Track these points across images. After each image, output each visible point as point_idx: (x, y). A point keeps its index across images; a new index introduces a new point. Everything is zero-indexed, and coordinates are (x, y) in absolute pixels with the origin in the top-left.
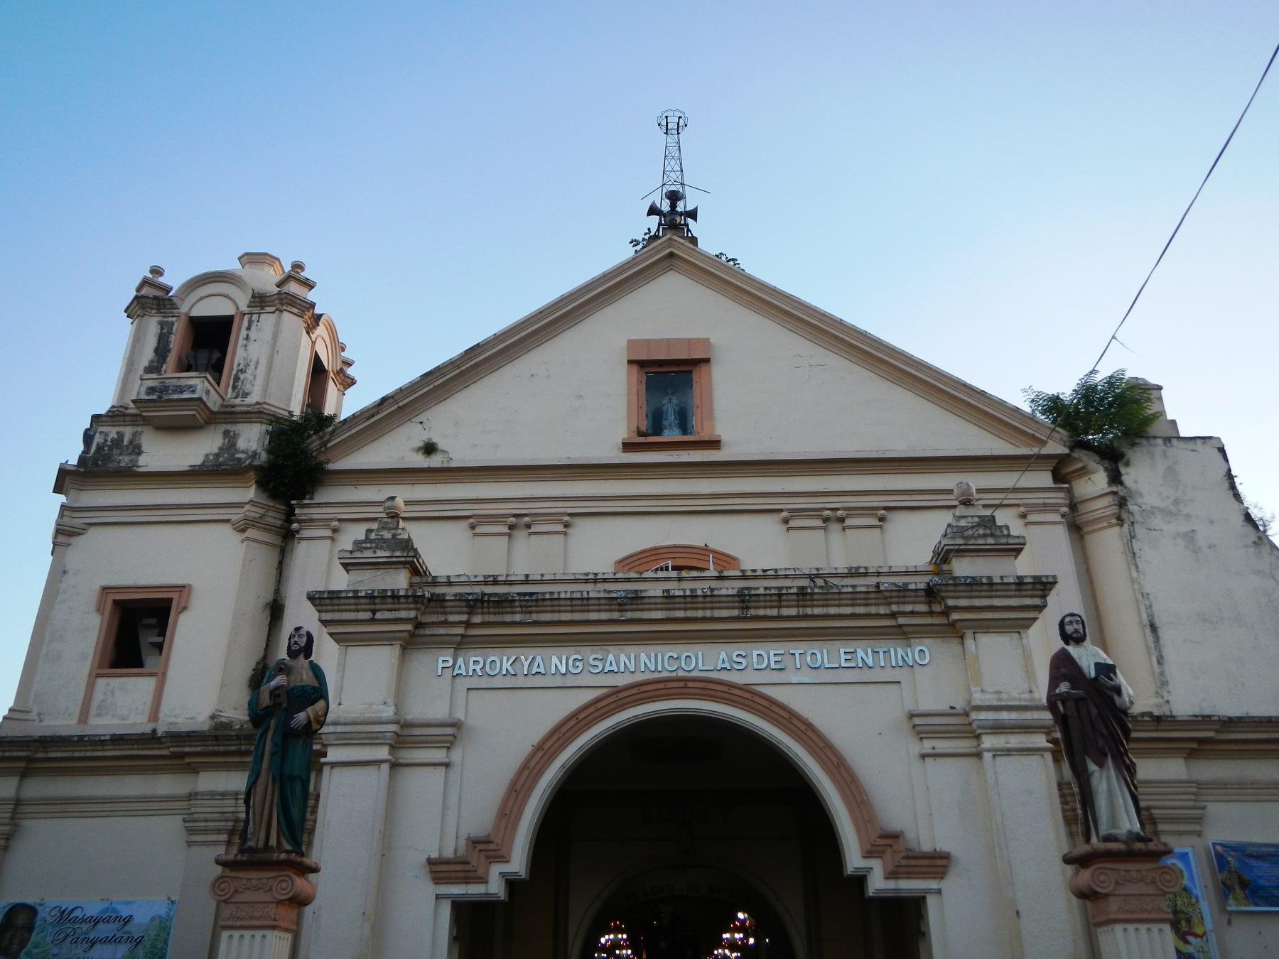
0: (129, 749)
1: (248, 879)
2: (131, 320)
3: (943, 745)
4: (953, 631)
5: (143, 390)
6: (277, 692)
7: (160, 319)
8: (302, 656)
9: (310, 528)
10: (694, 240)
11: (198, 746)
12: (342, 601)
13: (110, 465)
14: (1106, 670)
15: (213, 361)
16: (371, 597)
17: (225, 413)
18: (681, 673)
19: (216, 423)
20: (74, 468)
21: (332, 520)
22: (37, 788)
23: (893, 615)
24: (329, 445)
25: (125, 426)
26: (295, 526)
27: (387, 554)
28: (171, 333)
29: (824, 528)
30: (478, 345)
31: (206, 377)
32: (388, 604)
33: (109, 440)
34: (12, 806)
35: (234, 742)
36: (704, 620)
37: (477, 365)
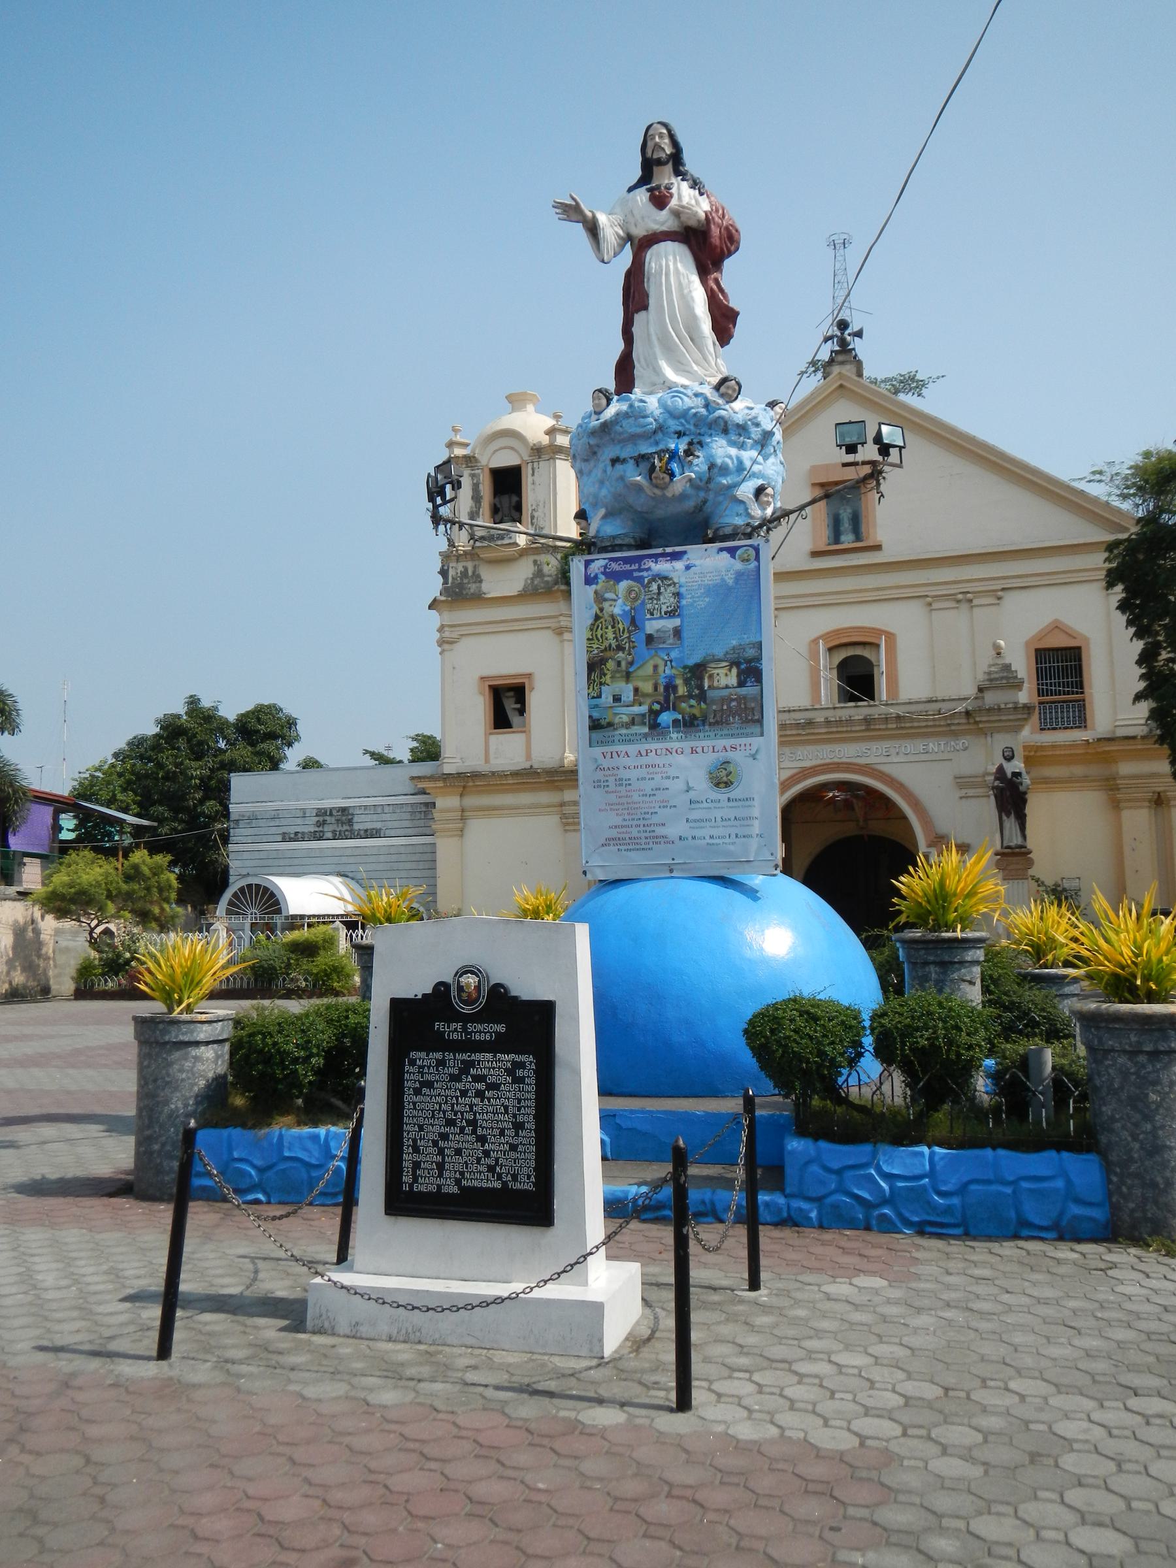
3: (971, 792)
4: (983, 732)
10: (859, 365)
14: (1017, 775)
15: (513, 503)
18: (836, 760)
22: (471, 801)
23: (949, 725)
29: (957, 608)
36: (847, 732)
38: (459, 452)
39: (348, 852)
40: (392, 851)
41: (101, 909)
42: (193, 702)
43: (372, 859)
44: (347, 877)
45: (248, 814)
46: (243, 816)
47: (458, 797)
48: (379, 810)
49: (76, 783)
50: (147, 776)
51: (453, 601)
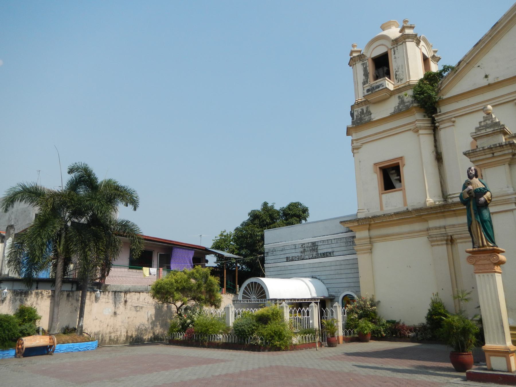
0: (401, 217)
1: (480, 257)
2: (352, 67)
5: (365, 91)
6: (470, 192)
7: (361, 63)
8: (474, 178)
9: (445, 123)
11: (425, 212)
12: (478, 152)
13: (362, 121)
16: (490, 148)
17: (396, 90)
19: (394, 95)
20: (352, 126)
21: (452, 118)
22: (375, 232)
24: (441, 89)
25: (363, 106)
26: (437, 124)
27: (492, 129)
28: (367, 67)
30: (497, 23)
31: (386, 79)
32: (498, 149)
33: (359, 112)
34: (369, 240)
35: (439, 209)
37: (499, 32)
38: (355, 55)
39: (317, 265)
40: (338, 263)
41: (173, 297)
42: (265, 204)
43: (328, 268)
44: (316, 278)
45: (271, 249)
46: (270, 250)
47: (367, 231)
48: (330, 242)
49: (214, 242)
50: (242, 237)
51: (356, 127)
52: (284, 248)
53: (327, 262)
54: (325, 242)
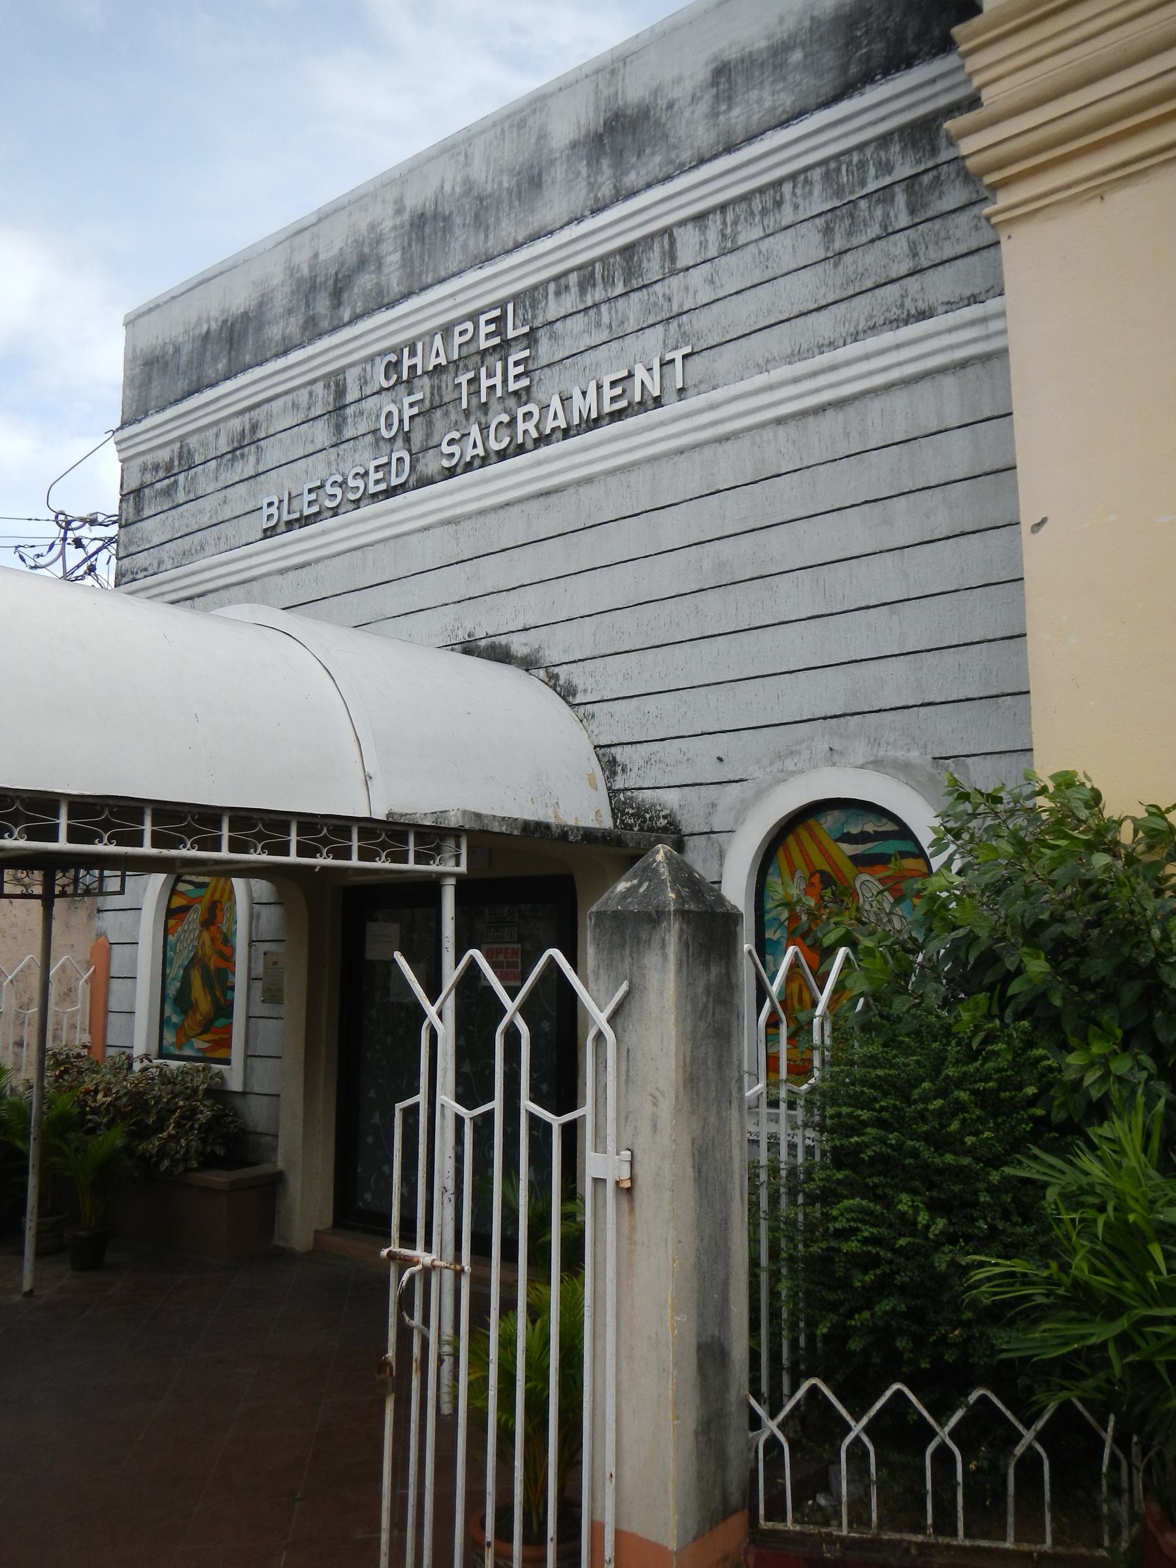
39: (512, 530)
45: (164, 455)
52: (254, 428)
53: (612, 472)
54: (608, 281)
